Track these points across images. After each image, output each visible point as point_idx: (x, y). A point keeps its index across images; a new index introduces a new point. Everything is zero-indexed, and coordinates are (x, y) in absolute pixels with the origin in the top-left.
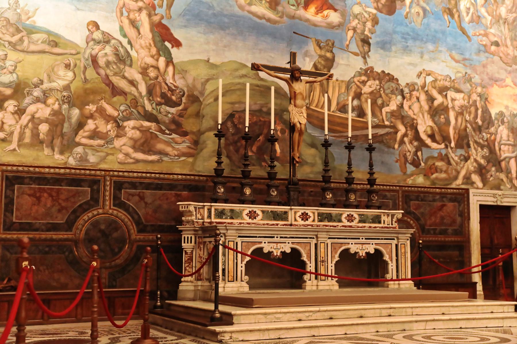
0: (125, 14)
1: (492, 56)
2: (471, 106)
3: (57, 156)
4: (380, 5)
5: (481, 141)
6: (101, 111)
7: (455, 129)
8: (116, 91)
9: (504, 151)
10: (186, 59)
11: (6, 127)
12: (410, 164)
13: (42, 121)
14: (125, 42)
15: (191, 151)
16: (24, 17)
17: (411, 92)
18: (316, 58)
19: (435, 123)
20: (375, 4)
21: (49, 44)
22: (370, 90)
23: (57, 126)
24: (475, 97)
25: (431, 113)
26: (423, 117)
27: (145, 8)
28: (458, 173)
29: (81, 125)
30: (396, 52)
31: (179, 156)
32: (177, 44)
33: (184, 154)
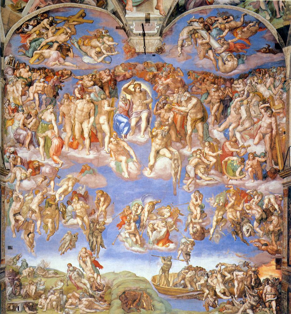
0: (81, 259)
2: (248, 277)
3: (59, 313)
4: (196, 237)
5: (254, 294)
6: (74, 296)
7: (237, 289)
8: (78, 288)
11: (42, 304)
14: (81, 269)
15: (108, 308)
16: (46, 266)
17: (212, 274)
18: (162, 265)
19: (226, 287)
20: (193, 237)
22: (191, 275)
23: (58, 302)
24: (250, 273)
26: (219, 284)
28: (239, 309)
29: (66, 301)
30: (204, 257)
32: (101, 267)
33: (105, 309)
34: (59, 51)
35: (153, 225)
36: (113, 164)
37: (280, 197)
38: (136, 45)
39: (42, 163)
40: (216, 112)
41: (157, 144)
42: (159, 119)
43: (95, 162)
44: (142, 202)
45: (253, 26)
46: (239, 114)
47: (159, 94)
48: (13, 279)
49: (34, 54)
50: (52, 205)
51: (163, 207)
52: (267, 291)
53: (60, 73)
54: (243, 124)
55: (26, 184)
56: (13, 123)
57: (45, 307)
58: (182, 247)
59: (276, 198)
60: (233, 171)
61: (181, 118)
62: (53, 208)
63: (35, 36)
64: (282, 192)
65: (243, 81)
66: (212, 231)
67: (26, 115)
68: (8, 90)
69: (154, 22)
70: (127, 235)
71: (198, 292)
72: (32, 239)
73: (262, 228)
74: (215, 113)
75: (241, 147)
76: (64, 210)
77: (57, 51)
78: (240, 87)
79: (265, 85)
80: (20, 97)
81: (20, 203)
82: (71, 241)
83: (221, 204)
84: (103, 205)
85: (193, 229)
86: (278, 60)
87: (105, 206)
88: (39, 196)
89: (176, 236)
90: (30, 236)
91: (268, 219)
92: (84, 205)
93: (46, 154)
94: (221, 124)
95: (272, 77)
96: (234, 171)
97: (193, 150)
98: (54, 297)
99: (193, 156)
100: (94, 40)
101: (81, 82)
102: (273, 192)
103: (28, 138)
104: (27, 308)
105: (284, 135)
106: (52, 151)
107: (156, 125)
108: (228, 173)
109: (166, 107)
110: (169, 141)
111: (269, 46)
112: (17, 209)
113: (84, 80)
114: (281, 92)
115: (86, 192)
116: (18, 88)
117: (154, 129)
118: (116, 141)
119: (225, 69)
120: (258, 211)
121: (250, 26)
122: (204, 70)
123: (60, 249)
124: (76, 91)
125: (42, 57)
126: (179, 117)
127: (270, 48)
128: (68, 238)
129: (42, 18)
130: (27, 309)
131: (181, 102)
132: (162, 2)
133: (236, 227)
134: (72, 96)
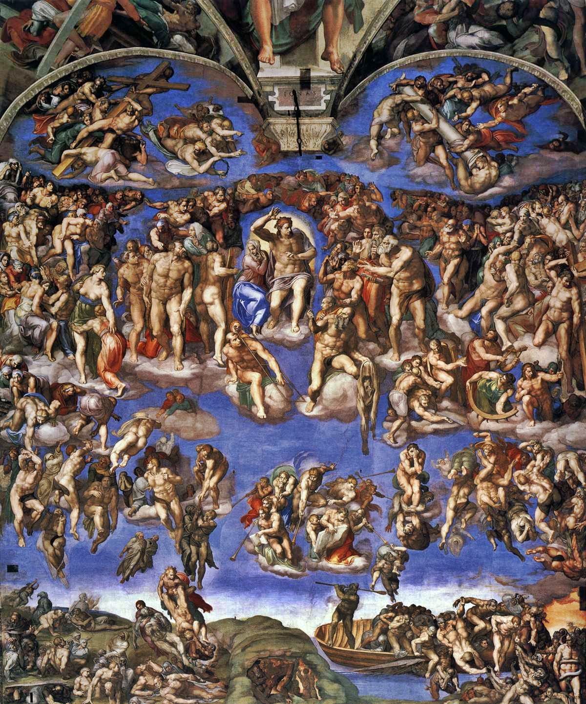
0: (165, 590)
1: (553, 572)
5: (535, 662)
6: (150, 669)
7: (500, 652)
8: (160, 652)
9: (565, 671)
10: (216, 620)
11: (83, 687)
12: (443, 690)
13: (107, 681)
14: (165, 613)
15: (223, 694)
18: (339, 602)
19: (475, 649)
20: (405, 542)
21: (109, 624)
22: (399, 624)
23: (117, 683)
26: (461, 644)
28: (503, 696)
29: (135, 681)
30: (429, 585)
31: (213, 699)
32: (208, 608)
33: (215, 697)
36: (232, 389)
38: (280, 135)
39: (80, 388)
41: (327, 346)
43: (195, 386)
44: (294, 469)
45: (532, 93)
46: (502, 281)
47: (330, 239)
48: (20, 635)
50: (103, 476)
51: (340, 480)
52: (562, 656)
53: (119, 196)
54: (510, 302)
55: (47, 431)
56: (17, 304)
57: (89, 694)
58: (380, 565)
60: (489, 401)
61: (378, 290)
62: (103, 482)
63: (65, 119)
65: (510, 210)
66: (445, 530)
67: (46, 287)
68: (6, 233)
69: (319, 86)
70: (263, 540)
71: (417, 660)
72: (59, 550)
73: (552, 524)
74: (450, 279)
75: (507, 350)
76: (129, 486)
77: (113, 151)
78: (504, 224)
79: (558, 220)
80: (34, 248)
81: (35, 472)
82: (143, 552)
83: (464, 473)
84: (210, 479)
85: (404, 526)
87: (215, 479)
88: (75, 457)
90: (55, 544)
91: (564, 504)
92: (170, 476)
93: (91, 367)
95: (572, 202)
97: (404, 358)
98: (107, 673)
99: (403, 371)
100: (190, 125)
101: (162, 215)
103: (51, 334)
104: (50, 696)
106: (102, 362)
107: (324, 306)
108: (479, 406)
109: (345, 268)
111: (566, 136)
113: (171, 211)
115: (176, 449)
116: (28, 229)
117: (320, 315)
118: (238, 340)
120: (543, 487)
121: (525, 93)
122: (428, 189)
123: (121, 570)
125: (81, 164)
126: (373, 288)
127: (568, 140)
128: (137, 546)
129: (80, 81)
130: (50, 699)
132: (335, 45)
133: (498, 521)
134: (146, 245)
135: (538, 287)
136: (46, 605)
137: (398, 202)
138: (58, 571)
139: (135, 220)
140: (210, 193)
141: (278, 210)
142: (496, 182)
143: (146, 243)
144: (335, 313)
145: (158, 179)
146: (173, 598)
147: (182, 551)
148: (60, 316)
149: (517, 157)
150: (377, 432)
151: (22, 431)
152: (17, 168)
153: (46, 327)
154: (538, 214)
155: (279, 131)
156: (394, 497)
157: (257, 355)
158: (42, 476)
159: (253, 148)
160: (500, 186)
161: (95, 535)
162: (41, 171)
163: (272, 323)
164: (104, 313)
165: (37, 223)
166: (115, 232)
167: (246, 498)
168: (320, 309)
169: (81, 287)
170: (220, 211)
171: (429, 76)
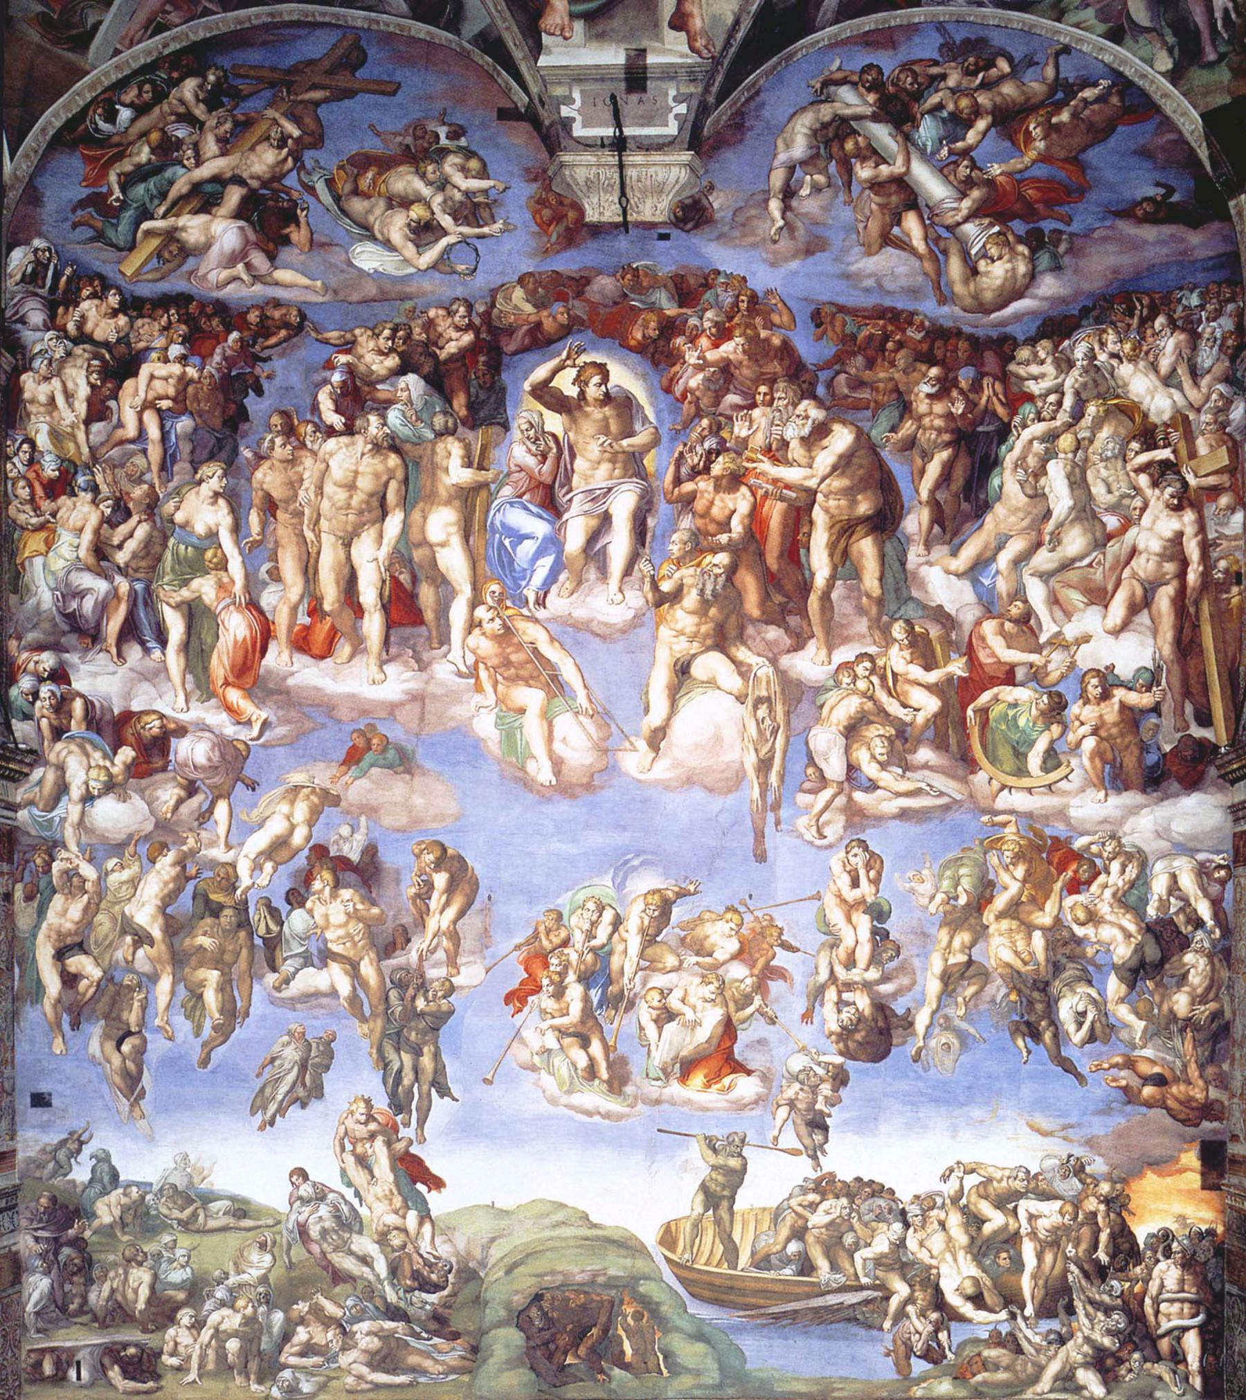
0: (349, 1147)
1: (1144, 1110)
2: (1082, 1224)
3: (254, 1387)
5: (1106, 1298)
6: (317, 1311)
7: (1035, 1277)
8: (338, 1277)
9: (1168, 1316)
11: (181, 1349)
13: (230, 1335)
14: (349, 1194)
16: (196, 1180)
18: (704, 1172)
19: (984, 1271)
22: (828, 1219)
23: (251, 1341)
24: (1091, 1204)
25: (975, 1250)
26: (955, 1260)
27: (381, 1133)
28: (1041, 1369)
29: (286, 1337)
31: (447, 1374)
32: (436, 1183)
34: (247, 220)
35: (664, 993)
36: (486, 727)
37: (1220, 867)
39: (175, 721)
40: (938, 486)
42: (686, 522)
43: (409, 715)
44: (612, 893)
45: (1099, 99)
46: (1038, 496)
48: (56, 1240)
49: (139, 234)
50: (221, 907)
51: (707, 916)
52: (1162, 1286)
53: (253, 317)
54: (1056, 540)
56: (49, 544)
58: (790, 1093)
59: (1203, 872)
61: (786, 516)
64: (1228, 845)
65: (1056, 347)
66: (922, 1020)
68: (27, 395)
69: (664, 85)
70: (551, 1041)
73: (1141, 1006)
74: (932, 492)
75: (1050, 643)
77: (241, 223)
78: (1043, 376)
79: (1154, 367)
80: (82, 427)
82: (303, 1066)
83: (963, 900)
85: (839, 1011)
86: (1212, 254)
87: (451, 912)
88: (166, 866)
89: (762, 1042)
90: (126, 1047)
91: (1167, 966)
92: (359, 906)
94: (962, 544)
95: (1183, 330)
96: (1020, 755)
98: (232, 1321)
99: (838, 684)
100: (401, 169)
101: (343, 359)
102: (1191, 845)
103: (117, 608)
105: (1235, 590)
106: (220, 665)
108: (994, 760)
109: (717, 468)
110: (733, 618)
112: (69, 926)
113: (360, 350)
114: (1221, 395)
115: (371, 851)
116: (70, 385)
117: (664, 571)
118: (498, 621)
119: (976, 297)
120: (1123, 929)
121: (1085, 100)
122: (888, 302)
123: (258, 1103)
124: (325, 401)
126: (775, 513)
127: (1176, 198)
128: (291, 1054)
129: (175, 75)
130: (115, 1373)
131: (785, 444)
133: (1031, 1003)
134: (308, 422)
135: (1112, 509)
136: (108, 1178)
137: (824, 332)
138: (132, 1105)
139: (285, 368)
140: (441, 312)
141: (579, 347)
142: (1027, 287)
143: (309, 417)
144: (699, 565)
145: (333, 281)
146: (363, 1162)
147: (385, 1065)
148: (136, 571)
149: (1071, 235)
150: (784, 813)
151: (58, 812)
152: (49, 260)
153: (108, 593)
154: (1114, 355)
155: (581, 180)
156: (819, 952)
157: (536, 651)
158: (98, 905)
159: (528, 216)
160: (1034, 297)
161: (207, 1031)
162: (97, 266)
163: (568, 585)
164: (223, 565)
165: (89, 373)
166: (247, 395)
167: (516, 954)
168: (667, 558)
169: (177, 508)
170: (460, 349)
171: (888, 63)
